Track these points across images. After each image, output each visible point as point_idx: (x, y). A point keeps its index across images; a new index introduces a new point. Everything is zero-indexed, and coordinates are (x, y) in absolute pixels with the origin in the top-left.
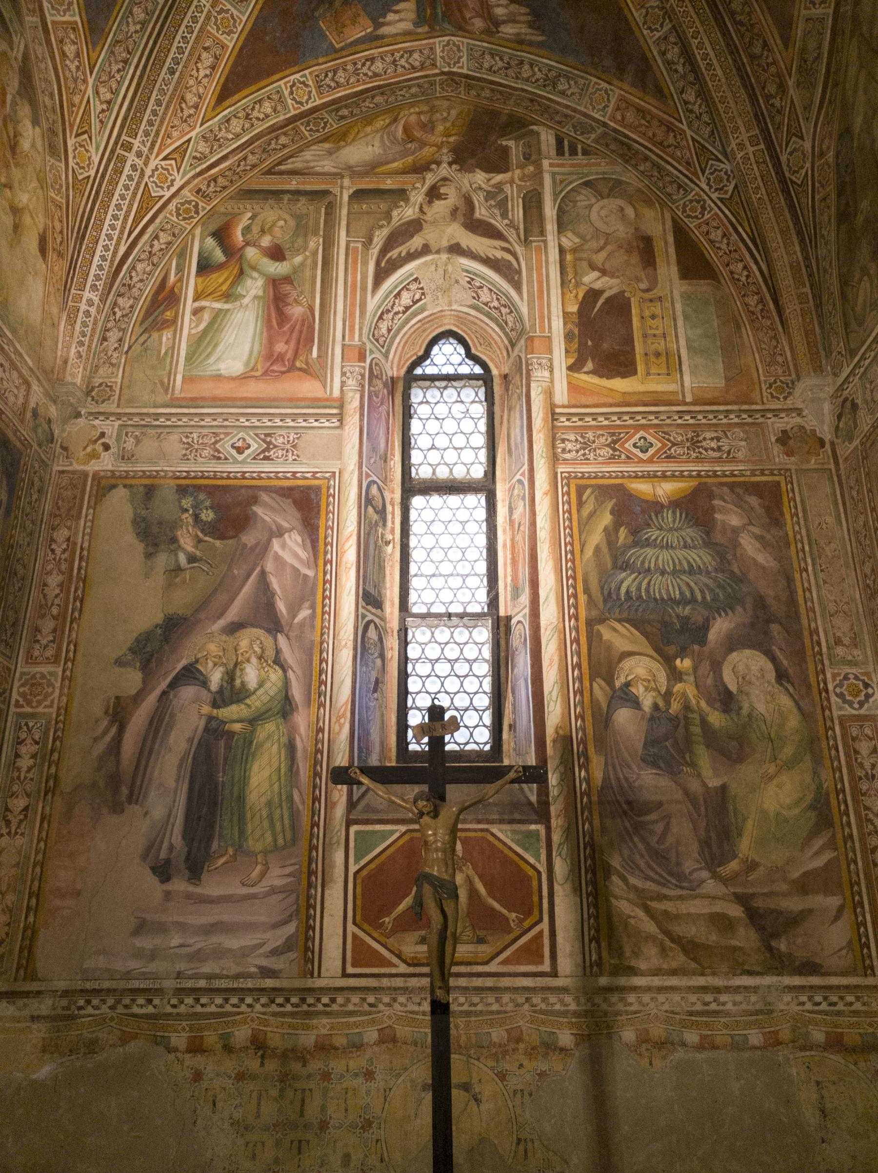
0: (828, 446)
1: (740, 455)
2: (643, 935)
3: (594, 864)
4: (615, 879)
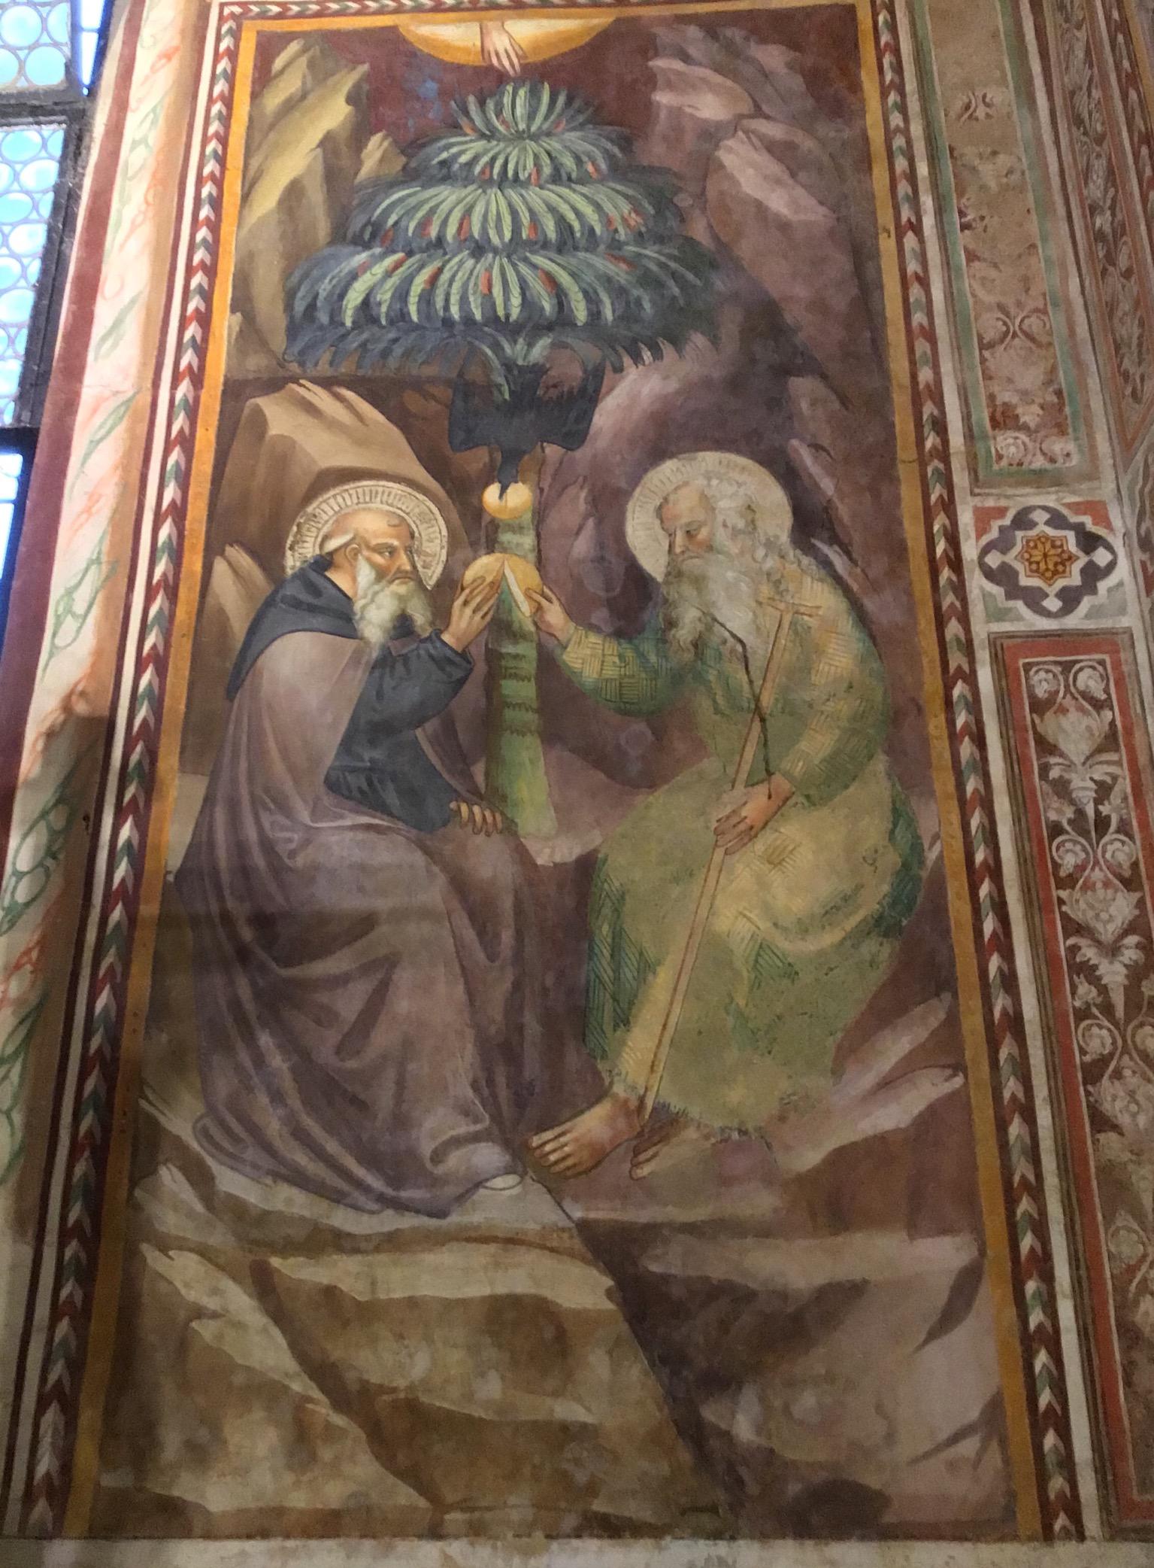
2: (239, 1379)
4: (170, 1178)
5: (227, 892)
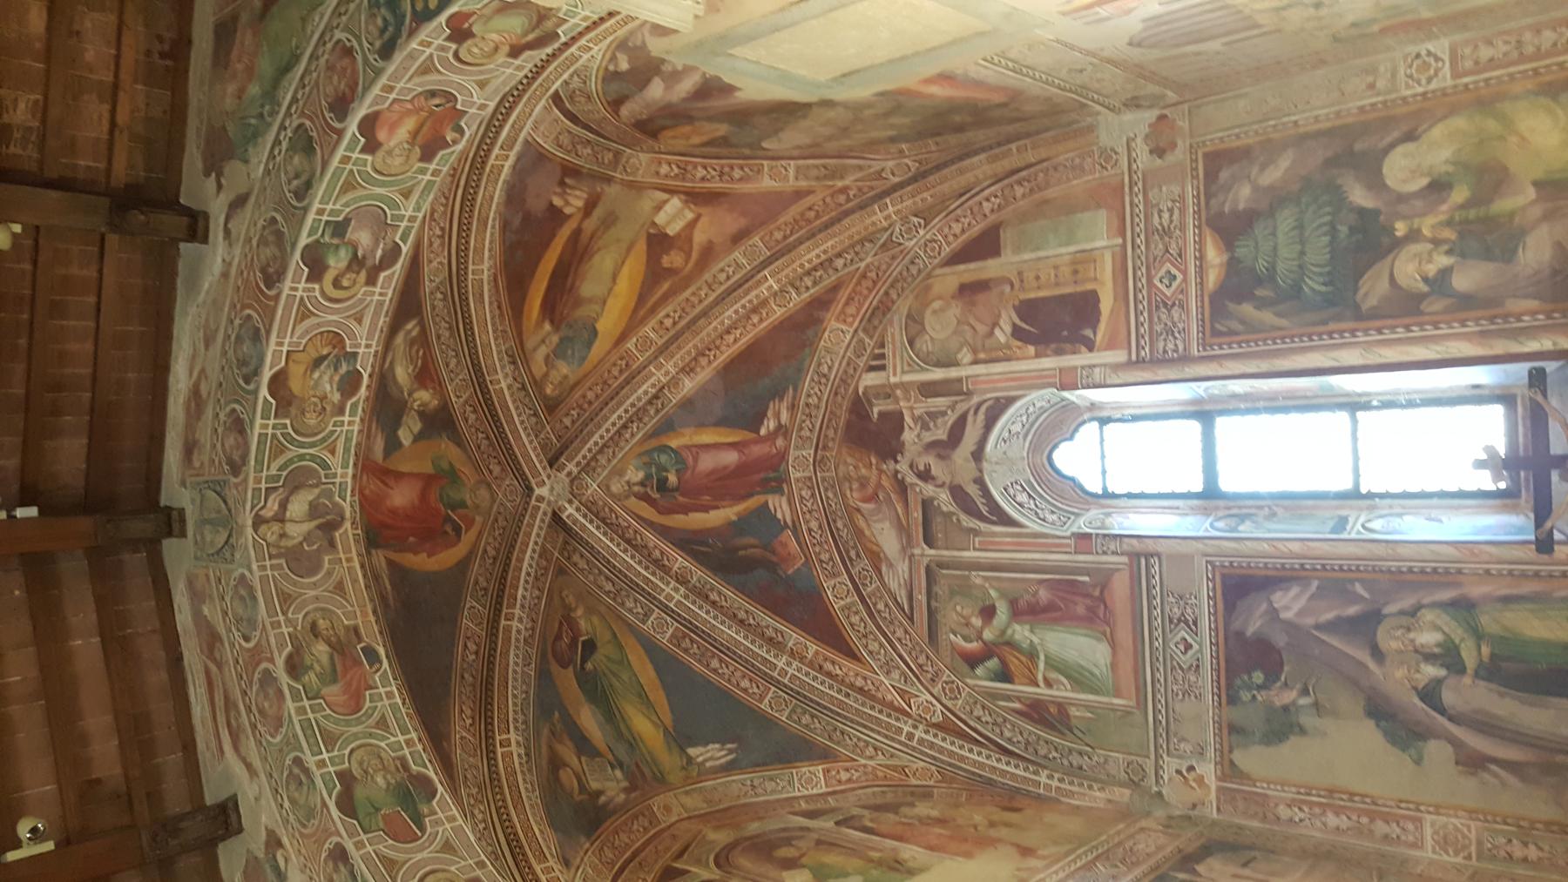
0: (1166, 112)
1: (1176, 190)
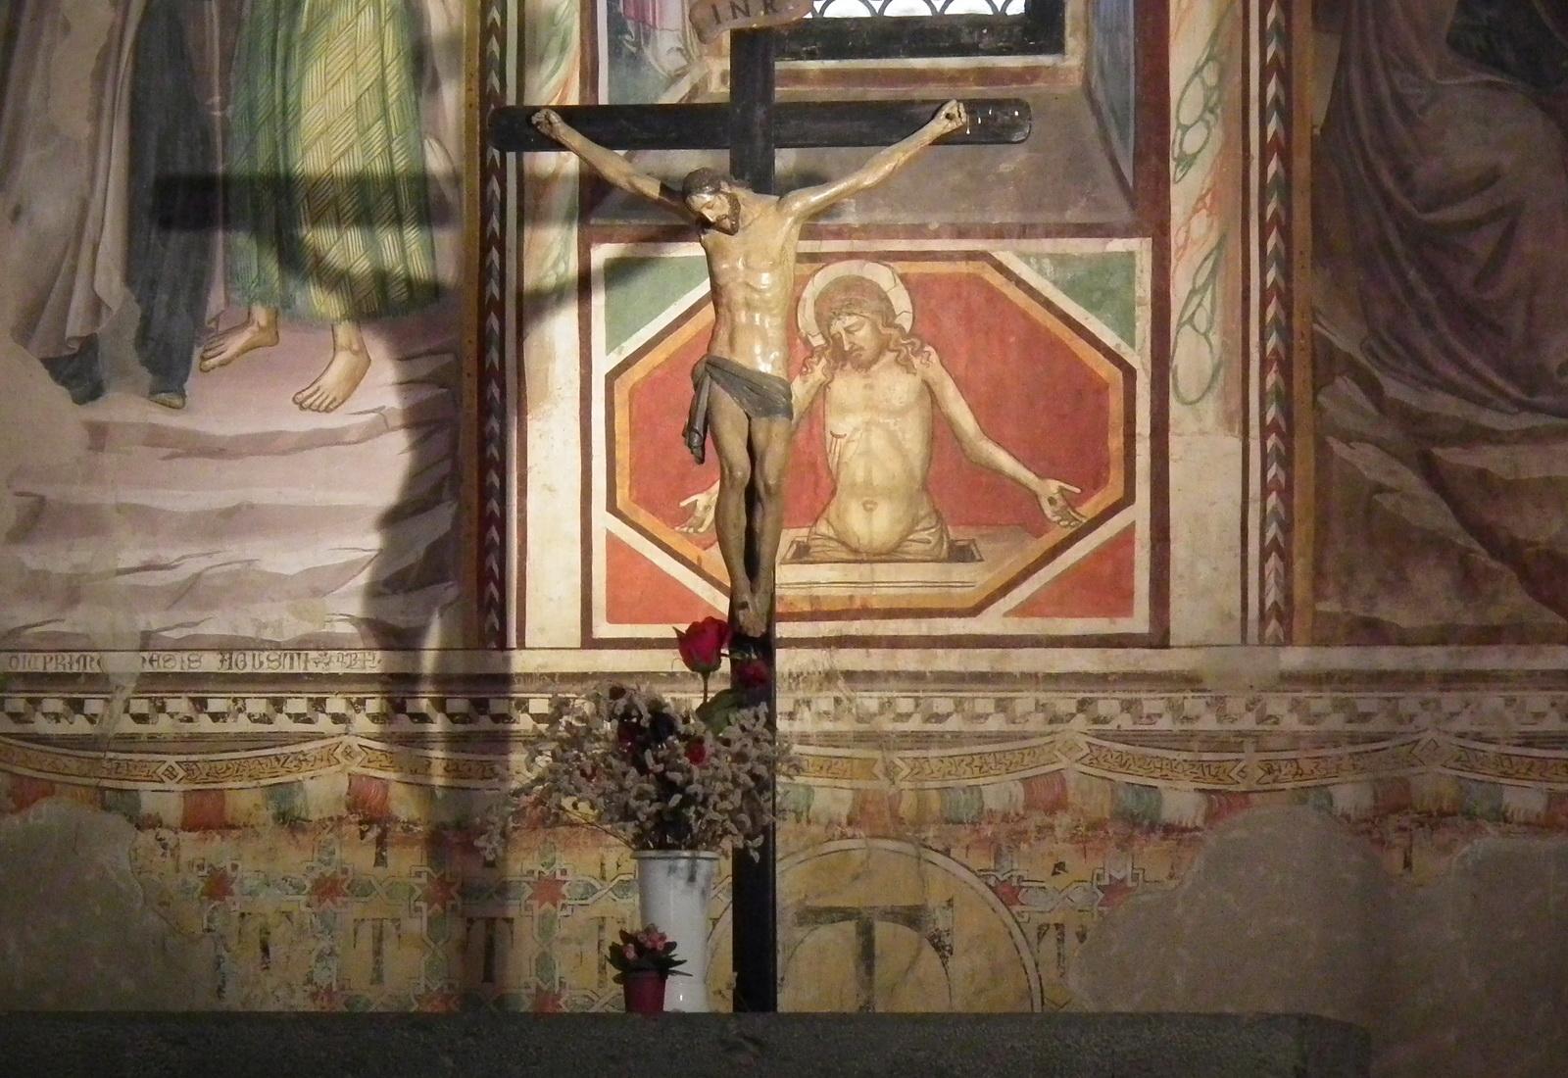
3: (1289, 348)
5: (1368, 147)
